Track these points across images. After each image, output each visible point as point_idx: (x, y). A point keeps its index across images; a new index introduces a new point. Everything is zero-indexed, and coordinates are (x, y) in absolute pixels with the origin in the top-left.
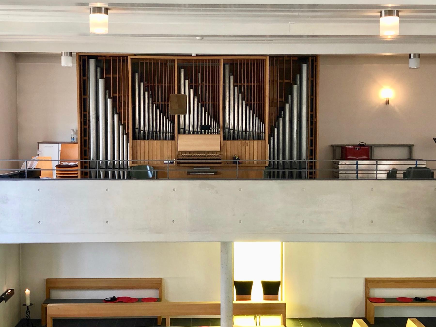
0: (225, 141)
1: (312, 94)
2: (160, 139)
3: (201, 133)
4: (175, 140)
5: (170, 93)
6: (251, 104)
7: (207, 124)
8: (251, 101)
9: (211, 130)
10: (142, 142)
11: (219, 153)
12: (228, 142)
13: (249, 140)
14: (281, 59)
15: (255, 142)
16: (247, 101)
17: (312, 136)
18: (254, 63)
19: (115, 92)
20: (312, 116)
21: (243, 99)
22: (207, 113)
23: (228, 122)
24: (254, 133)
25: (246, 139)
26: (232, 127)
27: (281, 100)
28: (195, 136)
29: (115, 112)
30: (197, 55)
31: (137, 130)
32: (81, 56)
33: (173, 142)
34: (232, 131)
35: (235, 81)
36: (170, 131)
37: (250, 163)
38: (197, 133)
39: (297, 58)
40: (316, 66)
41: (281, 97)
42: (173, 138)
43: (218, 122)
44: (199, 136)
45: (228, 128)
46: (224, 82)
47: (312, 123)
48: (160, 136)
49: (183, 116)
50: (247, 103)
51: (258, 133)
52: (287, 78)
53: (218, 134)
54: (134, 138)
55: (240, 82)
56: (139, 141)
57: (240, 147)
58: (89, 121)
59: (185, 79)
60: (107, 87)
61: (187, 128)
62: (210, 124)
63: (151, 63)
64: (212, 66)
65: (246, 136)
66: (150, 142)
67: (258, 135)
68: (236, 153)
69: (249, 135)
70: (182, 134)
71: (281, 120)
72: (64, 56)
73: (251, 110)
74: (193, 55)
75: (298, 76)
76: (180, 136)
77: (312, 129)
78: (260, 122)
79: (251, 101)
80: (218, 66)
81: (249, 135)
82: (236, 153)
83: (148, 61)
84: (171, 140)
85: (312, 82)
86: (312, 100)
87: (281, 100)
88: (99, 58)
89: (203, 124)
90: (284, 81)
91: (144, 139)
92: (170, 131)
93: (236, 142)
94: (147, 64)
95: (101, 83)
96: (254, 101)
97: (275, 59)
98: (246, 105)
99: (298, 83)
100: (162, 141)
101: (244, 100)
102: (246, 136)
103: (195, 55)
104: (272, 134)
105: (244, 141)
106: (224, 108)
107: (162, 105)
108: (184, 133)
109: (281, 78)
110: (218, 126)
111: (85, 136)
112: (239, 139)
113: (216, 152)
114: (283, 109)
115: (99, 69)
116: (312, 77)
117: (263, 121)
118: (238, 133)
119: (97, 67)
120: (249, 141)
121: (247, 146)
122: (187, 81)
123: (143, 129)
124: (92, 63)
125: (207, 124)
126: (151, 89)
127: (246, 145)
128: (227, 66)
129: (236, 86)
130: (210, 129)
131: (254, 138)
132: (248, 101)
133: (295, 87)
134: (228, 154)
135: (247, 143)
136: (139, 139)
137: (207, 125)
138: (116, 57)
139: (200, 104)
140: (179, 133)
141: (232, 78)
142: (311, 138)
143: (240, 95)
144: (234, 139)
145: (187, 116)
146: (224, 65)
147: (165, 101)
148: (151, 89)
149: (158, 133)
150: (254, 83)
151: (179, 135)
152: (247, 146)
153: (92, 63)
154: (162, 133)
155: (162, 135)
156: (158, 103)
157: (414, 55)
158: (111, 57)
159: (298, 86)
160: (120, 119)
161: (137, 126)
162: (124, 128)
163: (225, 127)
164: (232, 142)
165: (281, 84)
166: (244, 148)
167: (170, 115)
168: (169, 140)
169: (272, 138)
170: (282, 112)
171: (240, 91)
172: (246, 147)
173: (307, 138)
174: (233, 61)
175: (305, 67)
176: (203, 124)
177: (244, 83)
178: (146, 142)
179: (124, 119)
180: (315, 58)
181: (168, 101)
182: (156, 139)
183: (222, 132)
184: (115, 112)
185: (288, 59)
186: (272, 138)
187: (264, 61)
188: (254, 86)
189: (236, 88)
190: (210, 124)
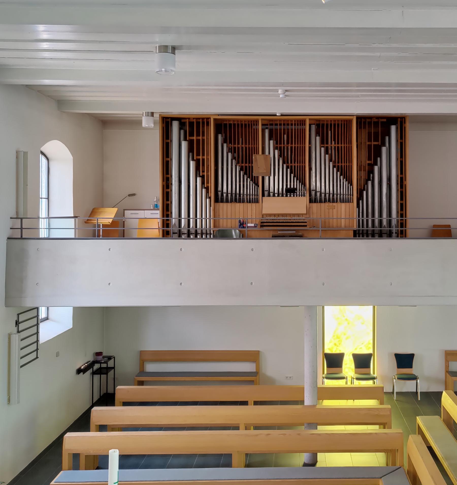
0: (311, 204)
1: (401, 157)
2: (243, 202)
3: (287, 196)
5: (254, 154)
6: (338, 166)
7: (292, 187)
8: (339, 163)
9: (297, 193)
10: (225, 205)
11: (305, 216)
12: (314, 205)
13: (336, 202)
14: (369, 120)
15: (343, 205)
16: (335, 162)
17: (402, 199)
18: (341, 124)
19: (198, 154)
20: (402, 179)
21: (330, 160)
22: (292, 175)
23: (314, 184)
24: (342, 196)
25: (333, 202)
26: (318, 189)
27: (369, 162)
28: (280, 198)
29: (198, 175)
30: (282, 115)
31: (220, 193)
32: (164, 119)
33: (257, 204)
35: (322, 142)
36: (254, 194)
37: (337, 227)
38: (283, 196)
39: (385, 120)
40: (405, 127)
41: (369, 159)
42: (257, 201)
43: (304, 184)
44: (284, 198)
45: (314, 190)
46: (310, 143)
47: (402, 187)
48: (243, 199)
49: (267, 178)
50: (335, 164)
51: (346, 196)
52: (376, 140)
53: (304, 196)
54: (216, 201)
55: (327, 143)
56: (221, 204)
58: (172, 184)
59: (270, 139)
61: (272, 190)
62: (295, 187)
63: (234, 125)
64: (298, 129)
65: (333, 199)
66: (233, 204)
67: (346, 198)
68: (323, 216)
69: (337, 198)
70: (266, 197)
71: (370, 183)
72: (145, 116)
73: (339, 171)
74: (277, 114)
75: (387, 138)
77: (402, 193)
78: (349, 183)
79: (339, 163)
80: (305, 129)
81: (337, 198)
82: (323, 216)
83: (232, 123)
84: (255, 202)
85: (401, 144)
86: (401, 162)
87: (369, 162)
89: (289, 187)
90: (373, 143)
91: (227, 201)
92: (254, 194)
93: (323, 204)
94: (230, 125)
96: (342, 163)
97: (363, 120)
98: (334, 167)
99: (387, 144)
100: (245, 204)
101: (332, 161)
102: (333, 199)
103: (280, 115)
104: (360, 197)
105: (331, 204)
106: (310, 169)
107: (246, 167)
108: (269, 195)
109: (370, 140)
110: (304, 188)
111: (168, 200)
112: (326, 201)
113: (302, 215)
114: (371, 171)
115: (182, 132)
116: (401, 138)
117: (351, 183)
118: (325, 195)
119: (180, 129)
120: (336, 204)
121: (335, 209)
122: (271, 142)
123: (226, 192)
125: (292, 187)
126: (235, 152)
127: (334, 208)
128: (313, 127)
129: (322, 147)
130: (296, 192)
131: (342, 201)
132: (335, 163)
133: (384, 150)
134: (315, 217)
135: (335, 206)
136: (222, 201)
137: (292, 188)
138: (199, 119)
139: (285, 166)
140: (263, 195)
141: (318, 138)
142: (402, 202)
143: (327, 156)
144: (321, 201)
146: (310, 125)
147: (249, 163)
148: (235, 152)
149: (242, 196)
150: (341, 144)
151: (263, 197)
152: (335, 209)
154: (245, 196)
155: (246, 198)
156: (242, 165)
158: (195, 119)
159: (387, 148)
160: (203, 183)
161: (220, 188)
162: (207, 192)
163: (312, 189)
164: (319, 204)
165: (370, 146)
166: (331, 210)
167: (255, 177)
168: (252, 202)
169: (361, 201)
170: (371, 175)
171: (327, 152)
172: (334, 210)
173: (397, 202)
174: (320, 122)
176: (289, 187)
177: (332, 145)
178: (229, 204)
179: (208, 183)
180: (404, 119)
181: (252, 163)
182: (240, 202)
184: (198, 175)
185: (376, 120)
186: (361, 201)
187: (350, 121)
188: (341, 147)
189: (323, 149)
190: (295, 187)
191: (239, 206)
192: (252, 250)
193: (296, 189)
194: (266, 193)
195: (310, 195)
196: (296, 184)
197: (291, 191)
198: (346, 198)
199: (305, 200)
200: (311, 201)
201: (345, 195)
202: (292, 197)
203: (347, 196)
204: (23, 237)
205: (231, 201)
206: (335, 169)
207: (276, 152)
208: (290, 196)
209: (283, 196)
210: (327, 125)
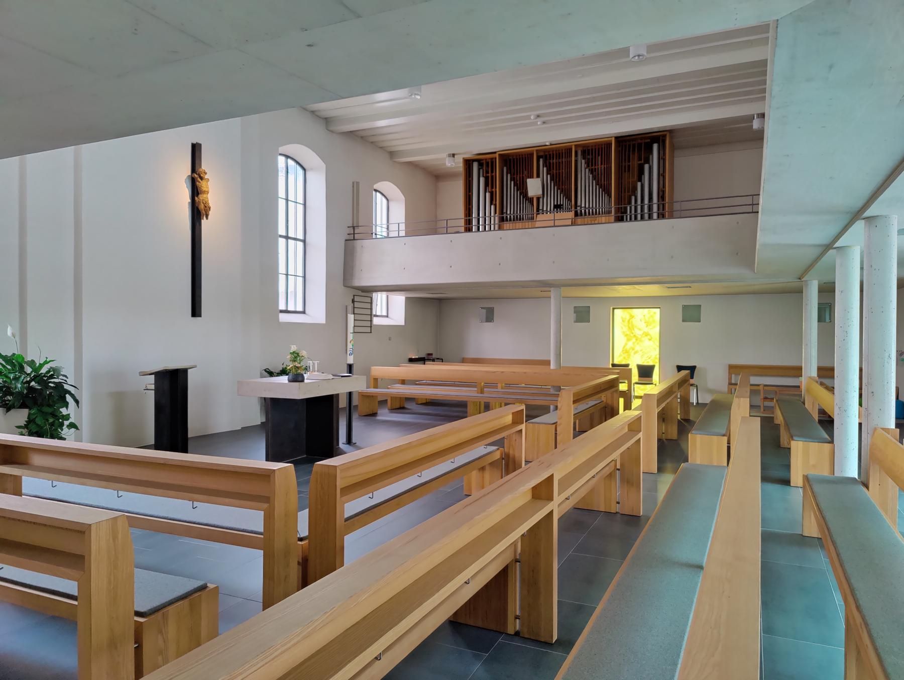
7: (559, 203)
9: (563, 208)
39: (649, 140)
60: (486, 185)
62: (562, 203)
76: (538, 215)
88: (481, 162)
95: (482, 180)
103: (549, 144)
114: (635, 188)
117: (610, 196)
124: (475, 166)
125: (559, 203)
153: (475, 166)
157: (758, 115)
175: (655, 146)
176: (556, 204)
183: (573, 212)
192: (501, 238)
193: (563, 205)
196: (563, 201)
197: (558, 207)
199: (571, 214)
200: (576, 215)
204: (355, 238)
205: (514, 220)
207: (549, 176)
210: (592, 150)
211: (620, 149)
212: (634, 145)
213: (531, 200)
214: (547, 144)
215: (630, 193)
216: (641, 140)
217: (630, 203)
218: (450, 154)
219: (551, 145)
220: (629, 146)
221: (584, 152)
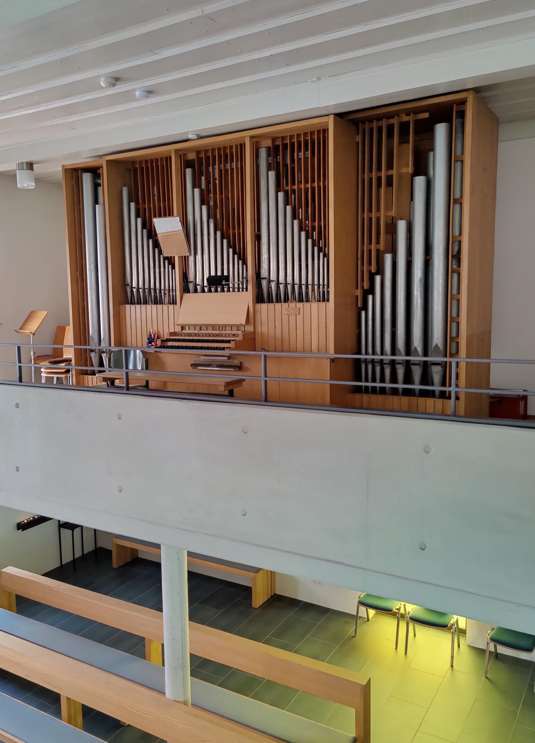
3: (210, 291)
4: (328, 300)
10: (133, 307)
12: (263, 307)
26: (273, 277)
34: (273, 285)
37: (304, 351)
44: (207, 295)
51: (324, 287)
57: (285, 318)
61: (199, 281)
62: (226, 274)
70: (192, 293)
76: (186, 295)
98: (301, 229)
102: (300, 293)
112: (288, 299)
125: (219, 274)
134: (265, 330)
140: (186, 290)
141: (272, 174)
145: (199, 257)
166: (292, 318)
172: (297, 316)
176: (213, 274)
191: (151, 309)
193: (228, 276)
194: (191, 286)
195: (259, 286)
198: (324, 292)
199: (248, 296)
200: (259, 298)
201: (321, 287)
202: (219, 294)
203: (326, 287)
206: (303, 234)
208: (216, 291)
209: (218, 292)
211: (359, 138)
212: (390, 128)
213: (170, 261)
214: (190, 137)
215: (382, 247)
216: (408, 114)
217: (380, 271)
218: (22, 163)
219: (200, 137)
220: (380, 129)
221: (273, 151)
